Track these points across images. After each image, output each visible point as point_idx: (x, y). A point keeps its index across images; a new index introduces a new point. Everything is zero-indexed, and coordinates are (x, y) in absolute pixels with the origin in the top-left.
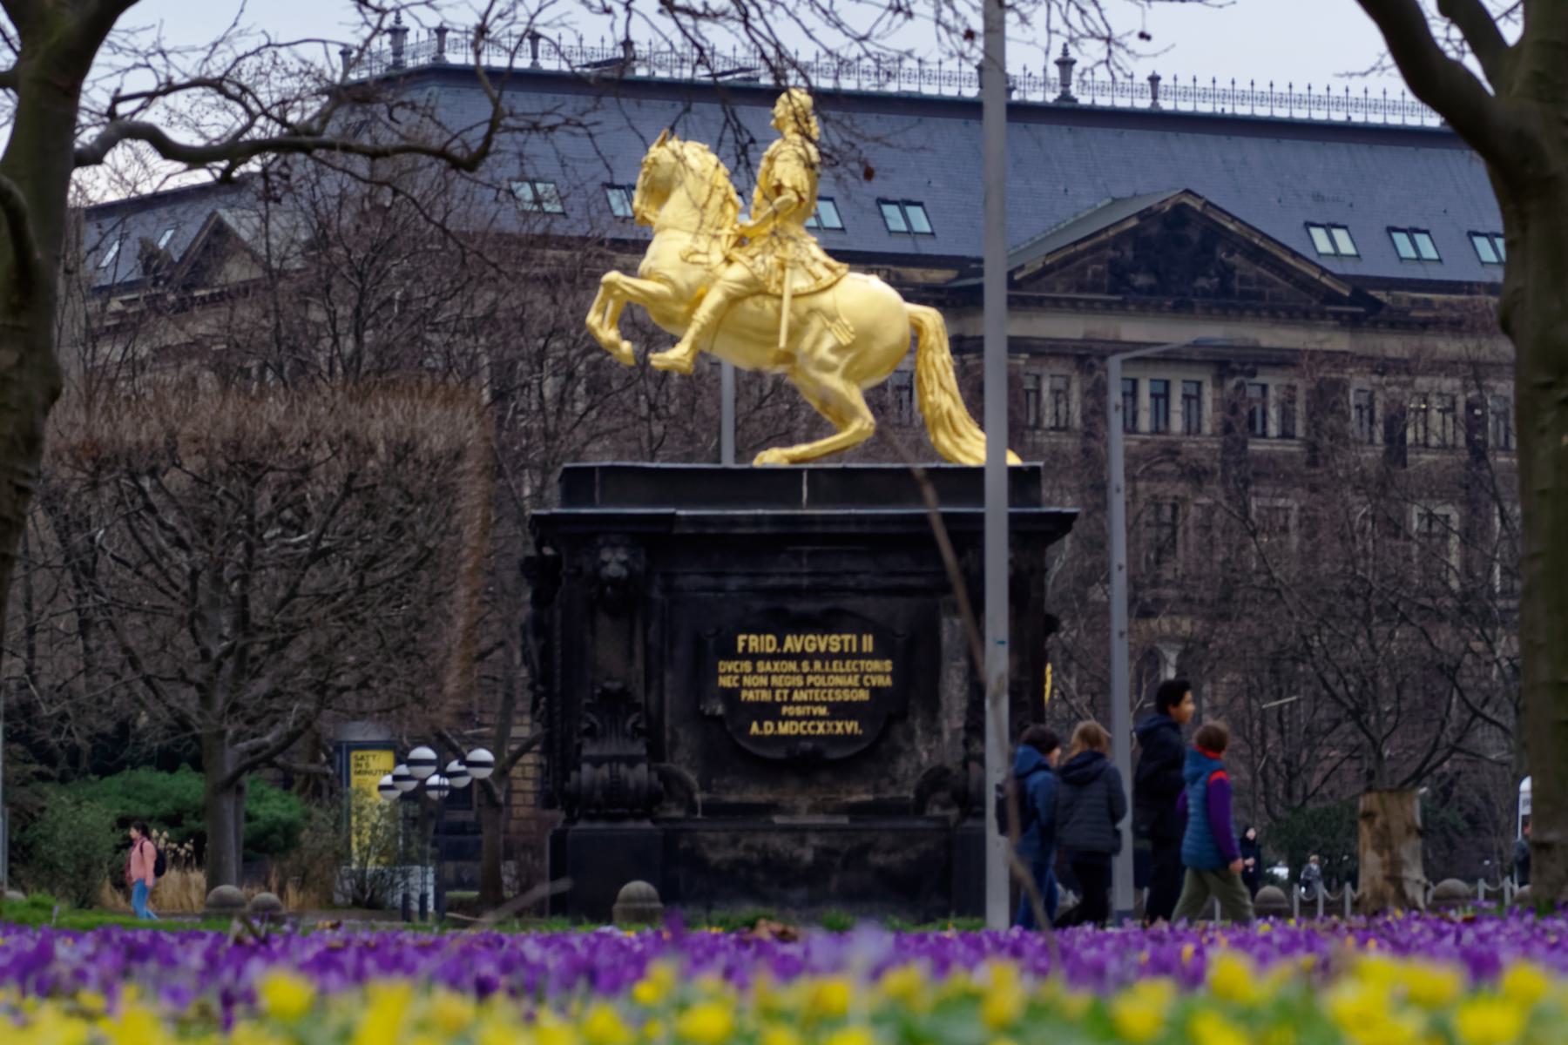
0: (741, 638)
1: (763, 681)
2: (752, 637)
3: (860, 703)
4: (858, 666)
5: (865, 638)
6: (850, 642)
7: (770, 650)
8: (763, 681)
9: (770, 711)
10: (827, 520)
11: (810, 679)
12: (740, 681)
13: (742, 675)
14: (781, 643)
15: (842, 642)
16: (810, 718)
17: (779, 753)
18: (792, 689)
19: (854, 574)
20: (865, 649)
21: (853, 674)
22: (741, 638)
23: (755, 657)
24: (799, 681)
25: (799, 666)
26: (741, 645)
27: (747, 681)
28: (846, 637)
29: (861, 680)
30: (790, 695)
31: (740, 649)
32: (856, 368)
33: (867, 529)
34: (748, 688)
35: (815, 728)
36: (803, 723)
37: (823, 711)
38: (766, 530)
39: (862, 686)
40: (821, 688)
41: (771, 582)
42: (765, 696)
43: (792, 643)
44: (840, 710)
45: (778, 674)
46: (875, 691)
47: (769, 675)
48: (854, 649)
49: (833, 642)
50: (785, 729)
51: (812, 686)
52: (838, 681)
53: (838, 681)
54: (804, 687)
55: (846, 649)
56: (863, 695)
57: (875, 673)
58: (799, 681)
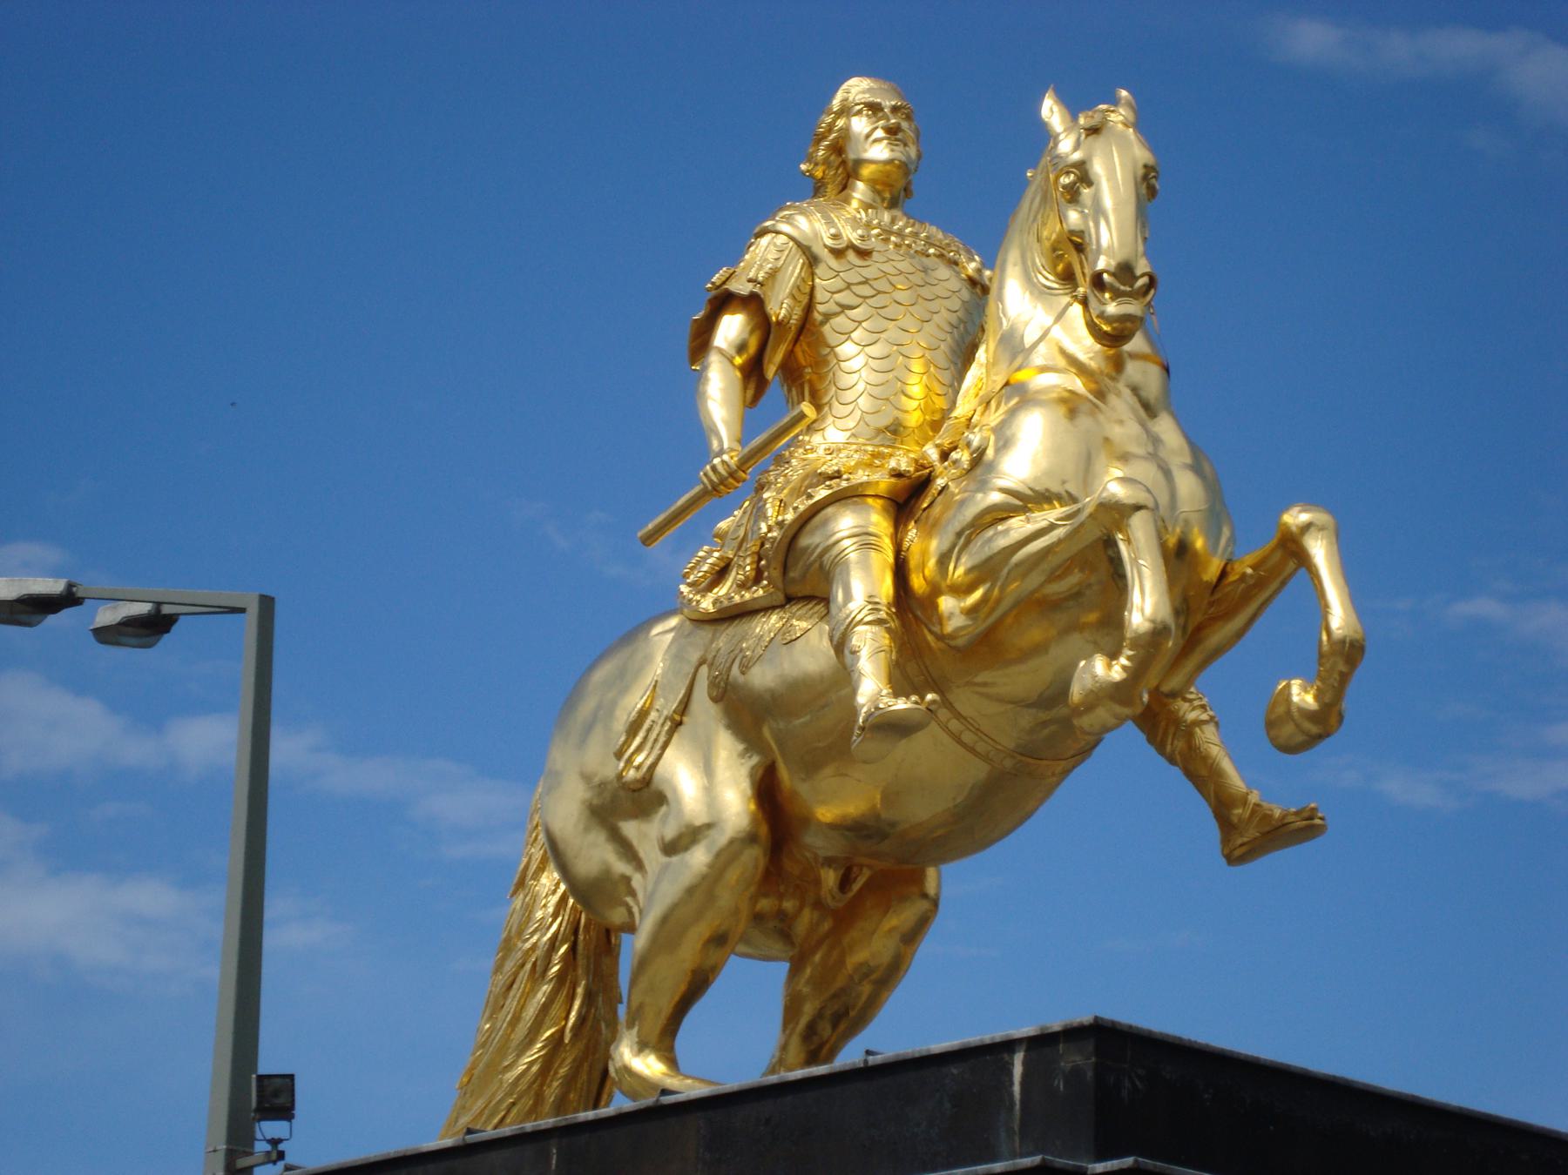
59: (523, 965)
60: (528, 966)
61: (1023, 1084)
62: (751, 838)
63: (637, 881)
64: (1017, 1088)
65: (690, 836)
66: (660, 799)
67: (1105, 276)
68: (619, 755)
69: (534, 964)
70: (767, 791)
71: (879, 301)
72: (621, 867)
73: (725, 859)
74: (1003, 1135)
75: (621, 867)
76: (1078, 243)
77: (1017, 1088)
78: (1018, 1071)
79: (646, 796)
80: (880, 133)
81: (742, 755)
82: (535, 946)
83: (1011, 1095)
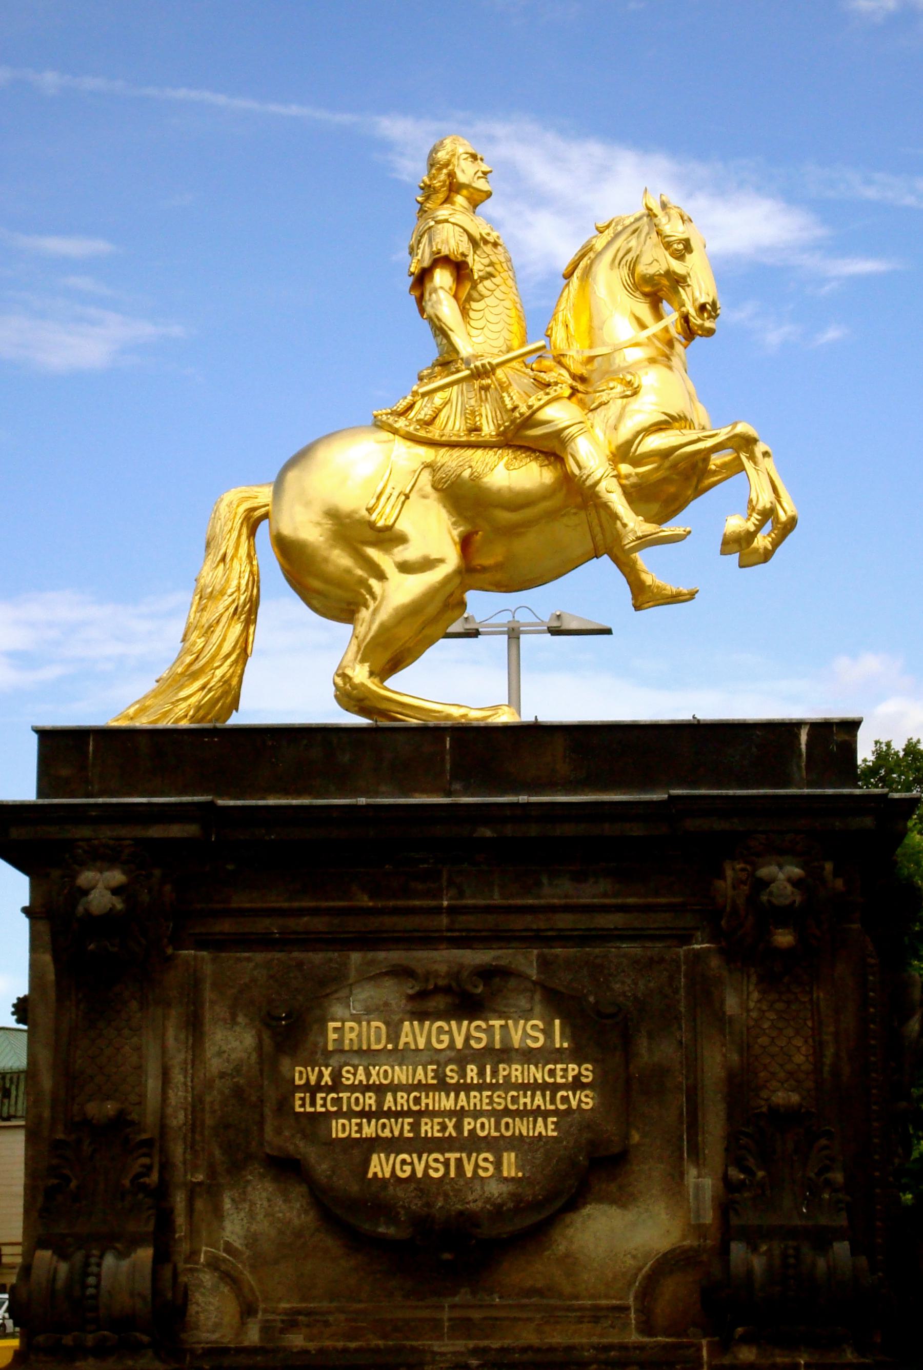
0: (332, 1025)
14: (394, 1034)
15: (489, 1030)
22: (332, 1025)
26: (332, 1036)
28: (497, 1023)
43: (414, 1034)
59: (227, 609)
60: (232, 610)
61: (806, 745)
62: (458, 572)
63: (373, 582)
64: (803, 747)
65: (427, 564)
66: (402, 539)
67: (708, 306)
68: (370, 510)
69: (236, 609)
70: (465, 544)
71: (503, 275)
72: (359, 572)
73: (448, 580)
74: (795, 769)
75: (359, 572)
76: (677, 281)
77: (803, 747)
78: (804, 738)
79: (389, 538)
80: (480, 174)
81: (454, 524)
82: (234, 601)
83: (800, 750)
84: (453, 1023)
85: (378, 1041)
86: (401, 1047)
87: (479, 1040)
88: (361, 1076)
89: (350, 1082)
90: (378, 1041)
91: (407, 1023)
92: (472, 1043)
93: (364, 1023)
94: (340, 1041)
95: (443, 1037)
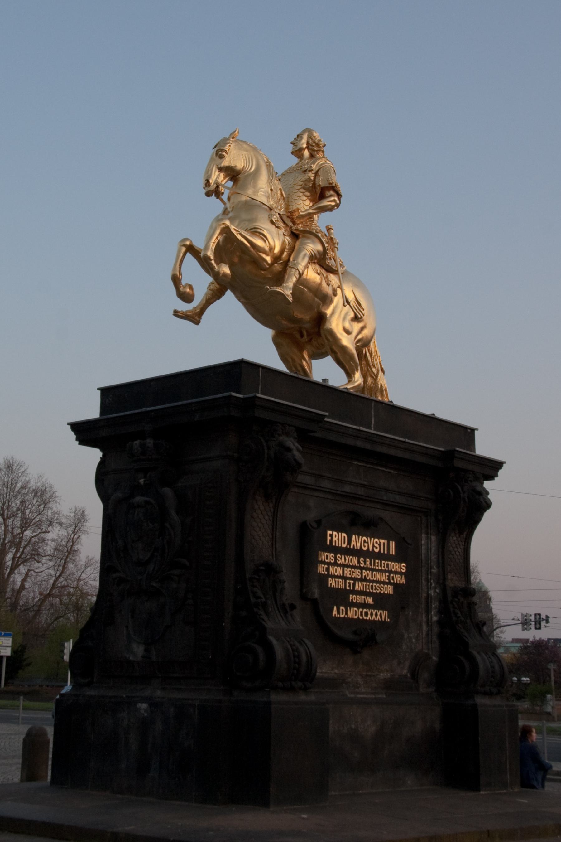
0: (329, 532)
1: (340, 571)
2: (335, 533)
3: (388, 595)
4: (388, 565)
5: (391, 542)
6: (384, 544)
7: (344, 546)
8: (340, 571)
9: (342, 597)
10: (392, 444)
11: (365, 573)
12: (328, 569)
13: (329, 564)
14: (349, 542)
15: (380, 545)
16: (364, 605)
17: (346, 634)
18: (355, 580)
19: (387, 490)
20: (391, 553)
21: (385, 571)
22: (329, 532)
23: (337, 550)
24: (356, 574)
25: (359, 562)
26: (329, 538)
27: (332, 570)
28: (382, 541)
29: (389, 576)
30: (354, 585)
31: (328, 543)
32: (360, 337)
33: (407, 456)
34: (334, 577)
35: (366, 614)
36: (361, 610)
37: (370, 600)
38: (359, 444)
39: (389, 583)
40: (370, 581)
41: (348, 489)
42: (341, 584)
44: (380, 601)
45: (348, 566)
46: (396, 586)
47: (343, 566)
48: (386, 552)
49: (374, 544)
50: (352, 613)
51: (365, 580)
52: (378, 576)
53: (378, 576)
54: (361, 580)
55: (382, 552)
56: (389, 590)
57: (396, 573)
58: (356, 574)
84: (369, 538)
85: (344, 543)
86: (352, 547)
87: (377, 548)
88: (343, 560)
89: (339, 562)
90: (344, 543)
91: (354, 536)
92: (375, 548)
93: (340, 534)
94: (331, 541)
95: (366, 544)
